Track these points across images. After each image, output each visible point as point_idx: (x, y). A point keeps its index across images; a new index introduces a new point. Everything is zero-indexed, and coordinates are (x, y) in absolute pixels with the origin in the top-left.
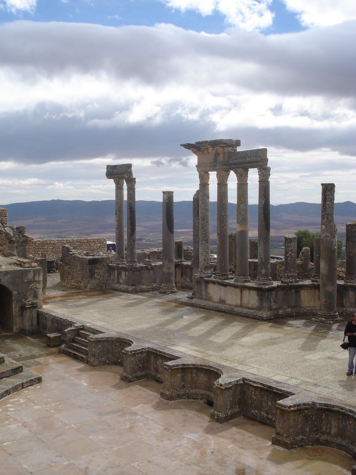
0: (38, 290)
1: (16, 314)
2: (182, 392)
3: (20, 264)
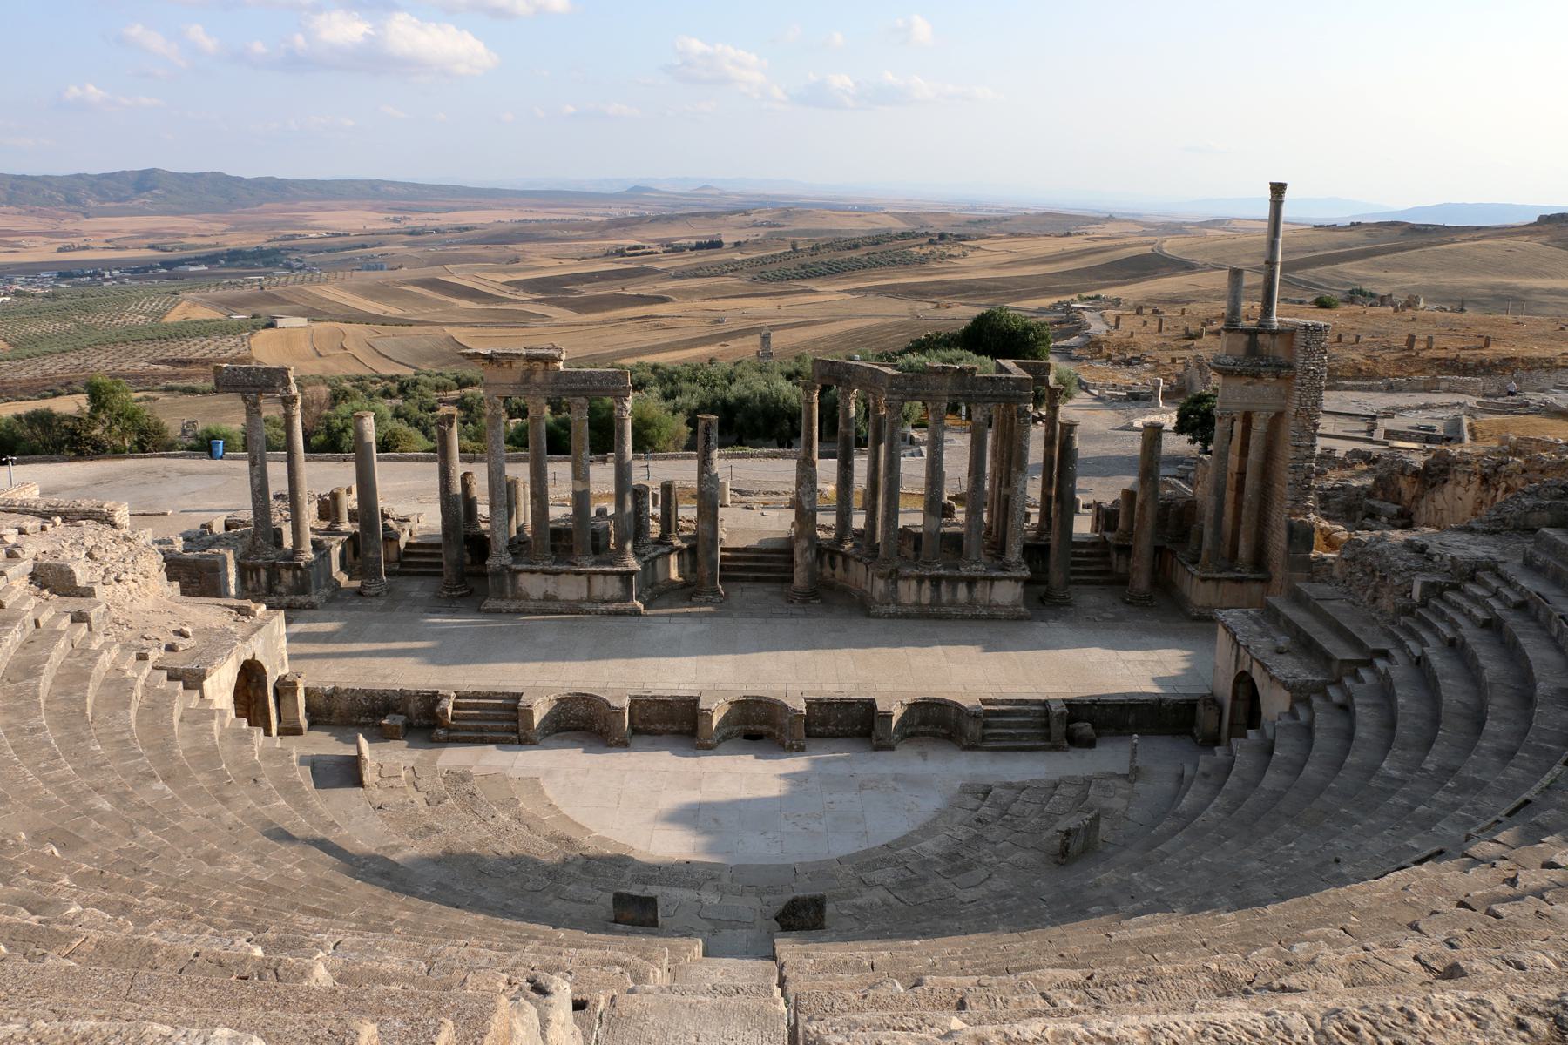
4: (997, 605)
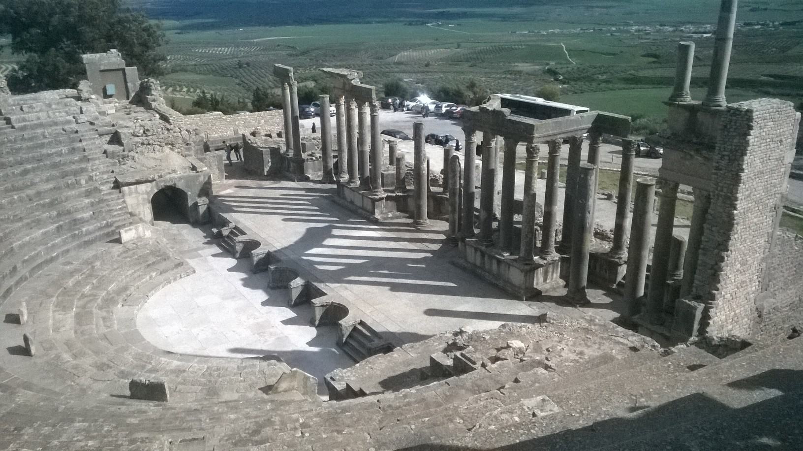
2: (279, 285)
3: (194, 168)
4: (511, 284)
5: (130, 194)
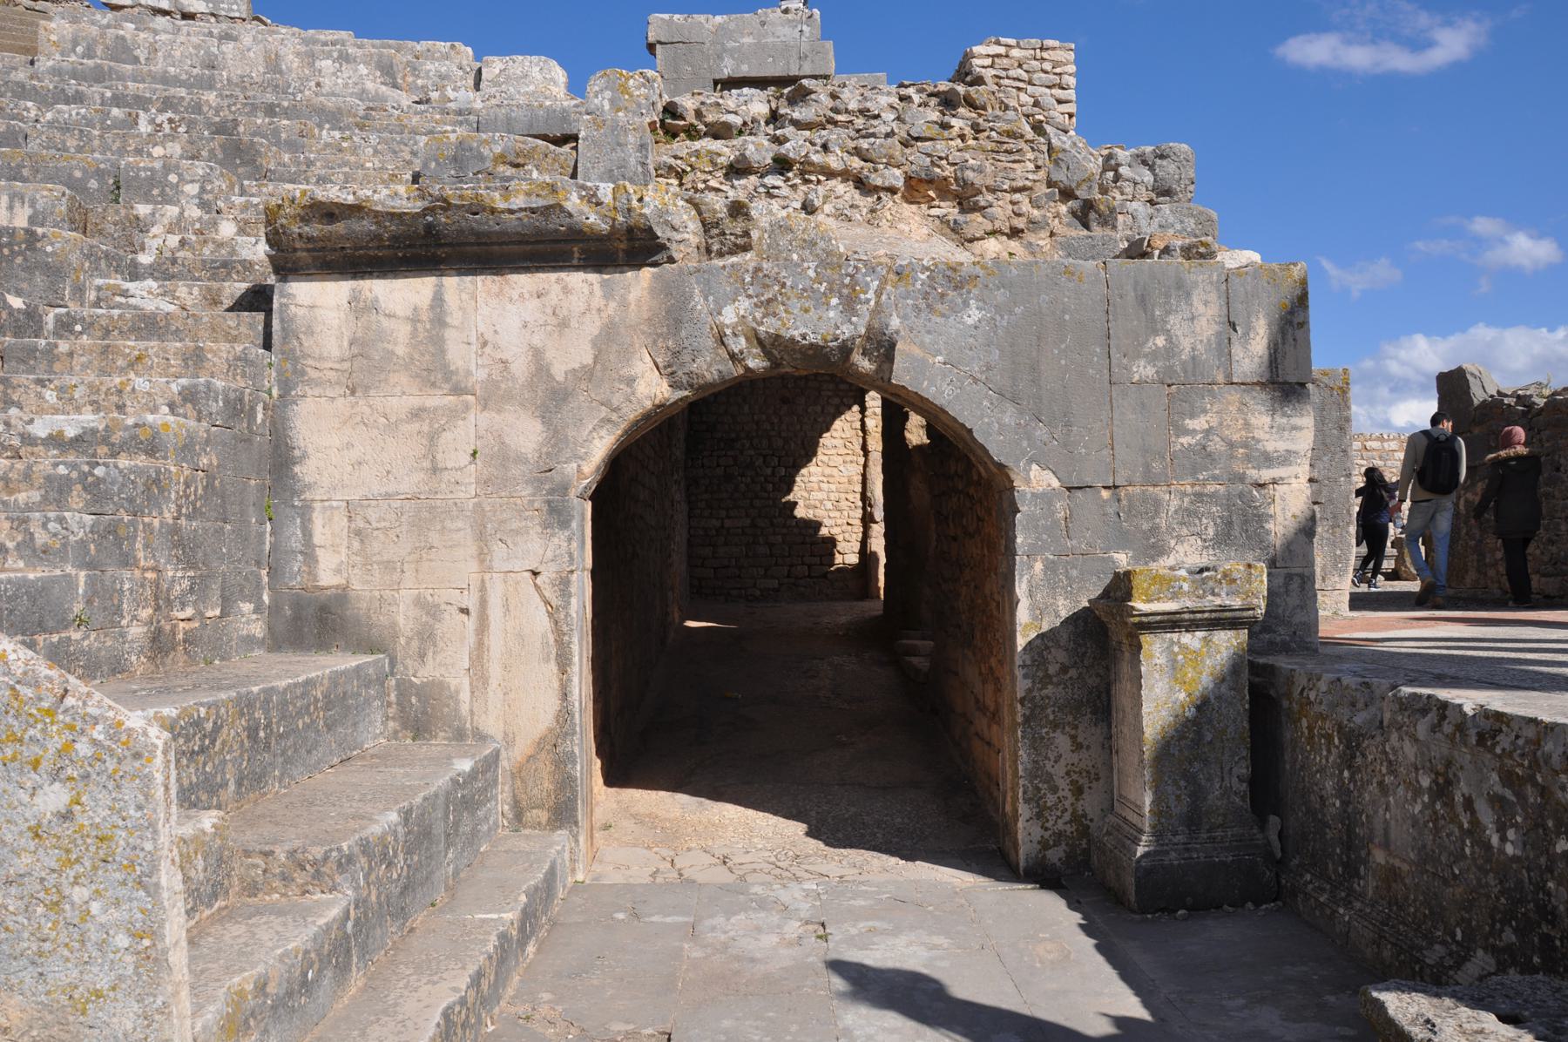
0: (1266, 475)
1: (1050, 690)
5: (364, 368)
